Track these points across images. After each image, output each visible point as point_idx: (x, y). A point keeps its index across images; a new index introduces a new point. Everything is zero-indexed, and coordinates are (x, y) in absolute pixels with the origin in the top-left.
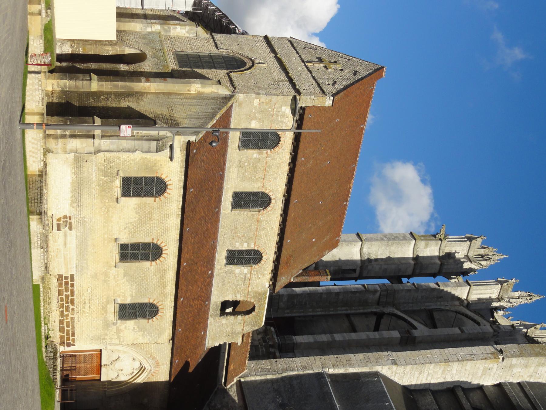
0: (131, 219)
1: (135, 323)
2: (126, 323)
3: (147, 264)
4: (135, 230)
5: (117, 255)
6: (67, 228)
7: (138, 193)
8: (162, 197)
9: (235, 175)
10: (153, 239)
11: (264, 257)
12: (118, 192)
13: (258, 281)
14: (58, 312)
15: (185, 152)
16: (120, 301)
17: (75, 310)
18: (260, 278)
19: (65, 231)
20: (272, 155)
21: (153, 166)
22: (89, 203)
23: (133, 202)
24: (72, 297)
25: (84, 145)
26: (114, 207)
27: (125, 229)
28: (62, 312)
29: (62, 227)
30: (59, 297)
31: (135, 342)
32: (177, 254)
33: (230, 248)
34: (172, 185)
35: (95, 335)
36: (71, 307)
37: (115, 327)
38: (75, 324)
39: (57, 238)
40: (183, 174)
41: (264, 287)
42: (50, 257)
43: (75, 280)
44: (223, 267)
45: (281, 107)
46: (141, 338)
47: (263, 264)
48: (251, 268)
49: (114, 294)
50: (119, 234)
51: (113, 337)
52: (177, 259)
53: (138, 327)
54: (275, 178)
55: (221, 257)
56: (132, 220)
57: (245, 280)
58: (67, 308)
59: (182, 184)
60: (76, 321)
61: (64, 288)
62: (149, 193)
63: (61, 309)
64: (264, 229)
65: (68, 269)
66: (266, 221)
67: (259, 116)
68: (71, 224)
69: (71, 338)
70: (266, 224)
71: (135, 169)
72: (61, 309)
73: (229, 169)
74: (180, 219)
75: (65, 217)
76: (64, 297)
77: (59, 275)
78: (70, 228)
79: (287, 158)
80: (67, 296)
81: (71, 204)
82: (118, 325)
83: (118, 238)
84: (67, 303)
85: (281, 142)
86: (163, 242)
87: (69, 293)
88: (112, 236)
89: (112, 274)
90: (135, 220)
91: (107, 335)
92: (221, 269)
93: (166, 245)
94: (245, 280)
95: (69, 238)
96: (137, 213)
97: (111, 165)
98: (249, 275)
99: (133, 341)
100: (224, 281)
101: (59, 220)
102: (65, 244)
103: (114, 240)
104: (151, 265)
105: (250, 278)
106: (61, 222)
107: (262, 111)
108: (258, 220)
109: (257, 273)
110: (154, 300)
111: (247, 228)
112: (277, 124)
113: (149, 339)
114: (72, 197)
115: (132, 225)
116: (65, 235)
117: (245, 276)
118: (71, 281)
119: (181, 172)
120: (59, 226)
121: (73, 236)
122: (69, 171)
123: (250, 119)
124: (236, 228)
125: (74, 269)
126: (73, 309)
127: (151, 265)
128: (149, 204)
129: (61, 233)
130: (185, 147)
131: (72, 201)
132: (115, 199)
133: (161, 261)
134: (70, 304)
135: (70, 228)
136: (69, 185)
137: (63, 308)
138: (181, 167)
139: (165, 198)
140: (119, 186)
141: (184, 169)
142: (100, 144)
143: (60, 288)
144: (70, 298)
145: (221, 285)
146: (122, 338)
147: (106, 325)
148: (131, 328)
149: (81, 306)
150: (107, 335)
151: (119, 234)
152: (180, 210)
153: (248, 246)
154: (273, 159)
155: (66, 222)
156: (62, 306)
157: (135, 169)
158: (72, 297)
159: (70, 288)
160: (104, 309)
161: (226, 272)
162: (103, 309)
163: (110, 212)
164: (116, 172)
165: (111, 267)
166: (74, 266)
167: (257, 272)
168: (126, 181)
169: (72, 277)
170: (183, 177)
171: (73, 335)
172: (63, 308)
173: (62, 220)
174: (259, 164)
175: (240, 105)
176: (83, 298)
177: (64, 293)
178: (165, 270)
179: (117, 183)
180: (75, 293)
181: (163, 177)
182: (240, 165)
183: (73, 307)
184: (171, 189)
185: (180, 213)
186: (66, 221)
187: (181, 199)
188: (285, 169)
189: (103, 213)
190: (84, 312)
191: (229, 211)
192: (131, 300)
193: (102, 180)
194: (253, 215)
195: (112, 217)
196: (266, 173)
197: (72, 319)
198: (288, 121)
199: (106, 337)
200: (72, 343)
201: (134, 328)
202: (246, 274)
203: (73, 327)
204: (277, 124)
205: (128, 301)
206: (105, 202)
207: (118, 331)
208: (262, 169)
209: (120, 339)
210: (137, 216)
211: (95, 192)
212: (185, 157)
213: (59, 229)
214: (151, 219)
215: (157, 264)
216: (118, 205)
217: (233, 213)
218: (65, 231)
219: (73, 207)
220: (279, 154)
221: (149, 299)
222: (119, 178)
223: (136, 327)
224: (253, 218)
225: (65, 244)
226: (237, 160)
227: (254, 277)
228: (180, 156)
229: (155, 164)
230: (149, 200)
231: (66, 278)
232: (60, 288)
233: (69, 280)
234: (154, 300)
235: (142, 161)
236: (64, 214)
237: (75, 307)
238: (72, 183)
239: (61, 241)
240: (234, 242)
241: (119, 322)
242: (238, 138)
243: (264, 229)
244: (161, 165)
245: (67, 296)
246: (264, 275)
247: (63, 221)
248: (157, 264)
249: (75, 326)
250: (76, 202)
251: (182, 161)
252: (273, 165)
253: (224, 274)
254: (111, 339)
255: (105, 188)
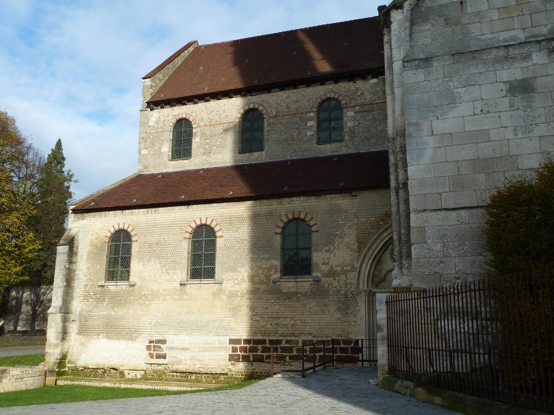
0: (159, 268)
1: (317, 251)
2: (317, 264)
3: (220, 242)
4: (171, 262)
5: (202, 282)
6: (162, 345)
7: (126, 263)
8: (132, 234)
9: (219, 156)
10: (185, 238)
11: (328, 96)
12: (122, 286)
13: (366, 94)
14: (294, 364)
15: (85, 215)
16: (277, 276)
17: (289, 338)
18: (362, 93)
19: (167, 348)
20: (198, 122)
21: (97, 247)
22: (133, 319)
23: (135, 265)
24: (267, 342)
25: (53, 324)
26: (140, 288)
27: (168, 274)
28: (291, 358)
29: (160, 353)
30: (265, 361)
31: (355, 247)
32: (207, 206)
33: (315, 140)
34: (119, 224)
35: (338, 308)
36: (284, 344)
37: (323, 280)
38: (315, 339)
39: (176, 360)
40: (107, 212)
41: (376, 84)
42: (202, 370)
43: (239, 338)
44: (344, 144)
45: (150, 126)
46: (347, 240)
47: (340, 95)
48: (345, 108)
49: (264, 284)
50: (175, 281)
51: (342, 282)
52: (215, 205)
53: (326, 246)
54: (224, 112)
55: (328, 150)
56: (158, 266)
57: (366, 111)
58: (284, 349)
59: (119, 212)
60: (310, 338)
61: (251, 354)
62: (128, 249)
63: (287, 359)
64: (288, 107)
65: (221, 348)
66: (277, 107)
67: (158, 145)
68: (158, 341)
69: (342, 346)
70: (281, 106)
71: (98, 267)
72: (287, 359)
73: (212, 164)
74: (160, 209)
75: (148, 348)
76: (265, 354)
77: (230, 360)
78: (164, 342)
79: (202, 105)
80: (265, 350)
81: (133, 340)
82: (319, 275)
83: (181, 281)
84: (276, 350)
85: (184, 116)
86: (190, 226)
87: (260, 347)
88: (177, 290)
89: (232, 287)
90: (158, 262)
91: (338, 292)
92: (347, 146)
93: (195, 221)
94: (366, 111)
95: (176, 345)
96: (149, 261)
97: (92, 294)
98: (357, 108)
99: (352, 250)
100: (366, 137)
101: (151, 356)
102: (185, 349)
103: (182, 287)
104: (221, 237)
105: (362, 105)
106: (155, 353)
107: (153, 144)
108: (276, 116)
109: (354, 99)
110: (278, 227)
111: (286, 127)
112: (166, 126)
113: (350, 227)
114: (125, 339)
115: (164, 266)
116: (172, 348)
117: (359, 112)
118: (240, 343)
119: (106, 216)
120: (159, 357)
121: (174, 339)
122: (95, 341)
123: (159, 154)
124: (286, 139)
125: (221, 338)
126: (288, 342)
127: (221, 237)
128: (140, 248)
129: (169, 354)
130: (79, 215)
131: (129, 339)
132: (130, 288)
133: (217, 224)
134: (279, 346)
135: (164, 342)
136: (111, 342)
137: (286, 356)
138: (101, 215)
139: (133, 229)
140: (115, 284)
141: (103, 213)
142: (55, 307)
143: (251, 359)
144: (267, 345)
145: (372, 141)
146: (345, 268)
147: (319, 291)
148: (326, 255)
149: (281, 330)
150: (338, 292)
151: (175, 281)
152: (150, 210)
153: (311, 120)
154: (202, 121)
155: (156, 347)
156: (282, 358)
157: (98, 267)
158: (267, 342)
159: (252, 345)
160: (289, 296)
161: (352, 138)
162: (289, 298)
163: (146, 293)
164: (100, 289)
165: (221, 289)
166: (216, 338)
167: (351, 99)
168: (111, 276)
169: (232, 341)
170: (111, 212)
171: (334, 342)
172: (286, 356)
173: (152, 352)
174: (208, 133)
175: (146, 167)
176: (269, 327)
177: (259, 353)
178: (231, 217)
179: (112, 286)
180: (260, 337)
181: (109, 235)
182: (208, 153)
183: (284, 342)
184: (124, 224)
185: (153, 210)
186: (154, 346)
187: (137, 210)
188: (213, 104)
189: (147, 302)
190: (293, 325)
191: (263, 153)
192: (275, 259)
193: (107, 305)
194: (269, 124)
195: (152, 290)
196: (218, 123)
197: (305, 343)
198: (163, 115)
199: (343, 292)
200: (352, 345)
201: (326, 251)
202: (355, 113)
203: (318, 342)
204: (166, 126)
205: (277, 263)
206: (134, 300)
207: (332, 274)
208: (213, 128)
209: (347, 271)
210: (153, 260)
211: (121, 312)
212: (90, 214)
213: (164, 357)
214: (157, 244)
215: (220, 230)
216: (138, 284)
217: (266, 148)
218: (166, 348)
219: (136, 337)
220: (196, 116)
221: (276, 233)
222: (106, 284)
223: (325, 249)
224: (273, 123)
225: (185, 349)
226: (202, 157)
227: (360, 101)
228: (88, 219)
229: (95, 245)
230: (135, 248)
231: (234, 350)
232: (251, 359)
233: (238, 346)
234: (278, 227)
235: (90, 260)
236: (145, 349)
237: (285, 338)
238: (109, 338)
239: (181, 355)
240: (305, 138)
241: (314, 274)
242: (178, 162)
243: (288, 107)
244: (96, 239)
245: (265, 350)
246: (357, 89)
247: (154, 350)
248: (220, 230)
249: (320, 339)
250: (131, 334)
251: (94, 216)
252: (209, 118)
253: (355, 140)
254: (346, 284)
255: (117, 300)
